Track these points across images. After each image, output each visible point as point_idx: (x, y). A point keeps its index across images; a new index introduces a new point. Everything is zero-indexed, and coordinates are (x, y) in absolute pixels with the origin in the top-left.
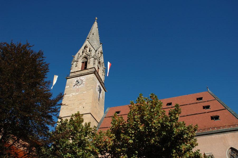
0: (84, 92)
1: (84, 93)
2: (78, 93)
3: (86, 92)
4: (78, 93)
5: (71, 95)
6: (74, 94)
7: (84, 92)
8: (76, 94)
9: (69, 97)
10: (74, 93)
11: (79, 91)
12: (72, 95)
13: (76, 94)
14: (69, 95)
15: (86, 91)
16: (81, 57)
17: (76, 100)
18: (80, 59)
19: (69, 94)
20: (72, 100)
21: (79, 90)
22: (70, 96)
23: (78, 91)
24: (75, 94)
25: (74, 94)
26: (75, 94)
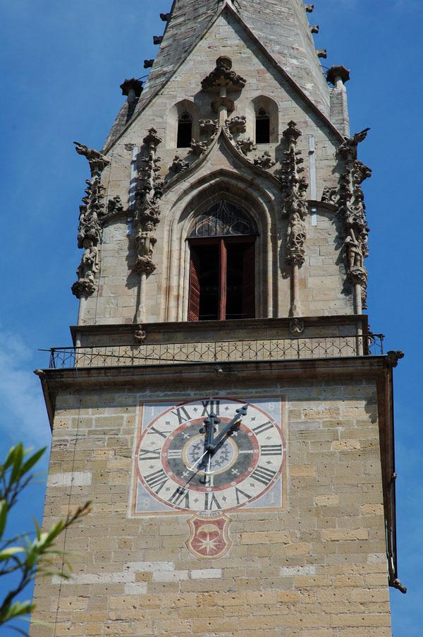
0: (290, 562)
1: (288, 582)
3: (311, 570)
4: (215, 573)
5: (129, 576)
6: (164, 570)
7: (287, 572)
8: (197, 574)
10: (169, 566)
11: (220, 546)
12: (144, 577)
13: (197, 574)
14: (105, 579)
16: (185, 185)
18: (172, 196)
21: (226, 534)
22: (118, 588)
23: (209, 544)
24: (183, 575)
25: (164, 570)
26: (183, 575)
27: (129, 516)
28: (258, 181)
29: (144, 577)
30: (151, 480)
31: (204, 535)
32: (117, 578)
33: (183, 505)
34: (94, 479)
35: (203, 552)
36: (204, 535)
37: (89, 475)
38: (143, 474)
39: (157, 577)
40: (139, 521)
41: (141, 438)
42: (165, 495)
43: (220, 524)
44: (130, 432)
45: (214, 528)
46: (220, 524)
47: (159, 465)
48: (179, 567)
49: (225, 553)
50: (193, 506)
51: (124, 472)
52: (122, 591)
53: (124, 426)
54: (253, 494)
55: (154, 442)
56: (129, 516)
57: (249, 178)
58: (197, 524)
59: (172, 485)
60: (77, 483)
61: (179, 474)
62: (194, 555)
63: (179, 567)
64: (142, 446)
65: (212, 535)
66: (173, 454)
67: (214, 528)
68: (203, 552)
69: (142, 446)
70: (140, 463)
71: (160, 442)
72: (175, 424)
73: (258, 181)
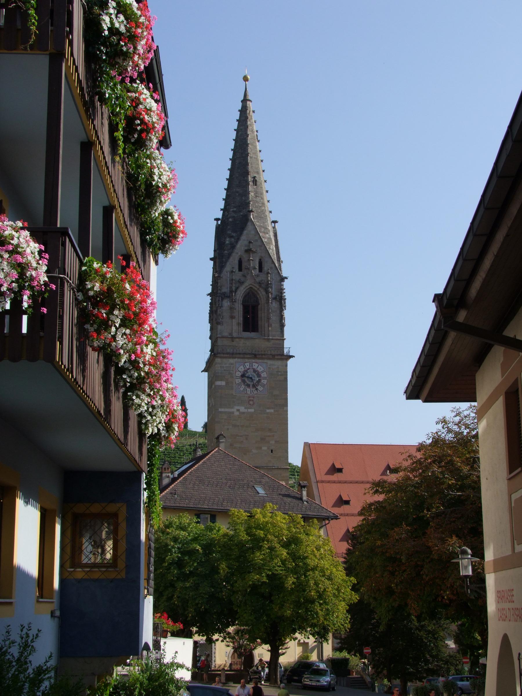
0: (269, 408)
2: (252, 410)
3: (272, 411)
4: (252, 410)
5: (234, 410)
6: (242, 409)
7: (268, 411)
8: (250, 410)
11: (254, 404)
12: (238, 410)
13: (250, 410)
15: (272, 408)
22: (233, 413)
23: (251, 403)
24: (246, 410)
25: (242, 409)
27: (234, 394)
29: (238, 410)
30: (239, 384)
31: (250, 400)
32: (231, 410)
34: (226, 384)
35: (250, 405)
36: (250, 400)
38: (237, 383)
39: (241, 411)
41: (236, 372)
42: (242, 389)
43: (254, 397)
44: (233, 371)
45: (252, 399)
46: (254, 397)
48: (245, 408)
52: (234, 414)
54: (261, 390)
58: (249, 397)
59: (243, 386)
61: (244, 383)
63: (245, 408)
64: (236, 375)
65: (252, 400)
68: (250, 405)
69: (236, 375)
70: (236, 380)
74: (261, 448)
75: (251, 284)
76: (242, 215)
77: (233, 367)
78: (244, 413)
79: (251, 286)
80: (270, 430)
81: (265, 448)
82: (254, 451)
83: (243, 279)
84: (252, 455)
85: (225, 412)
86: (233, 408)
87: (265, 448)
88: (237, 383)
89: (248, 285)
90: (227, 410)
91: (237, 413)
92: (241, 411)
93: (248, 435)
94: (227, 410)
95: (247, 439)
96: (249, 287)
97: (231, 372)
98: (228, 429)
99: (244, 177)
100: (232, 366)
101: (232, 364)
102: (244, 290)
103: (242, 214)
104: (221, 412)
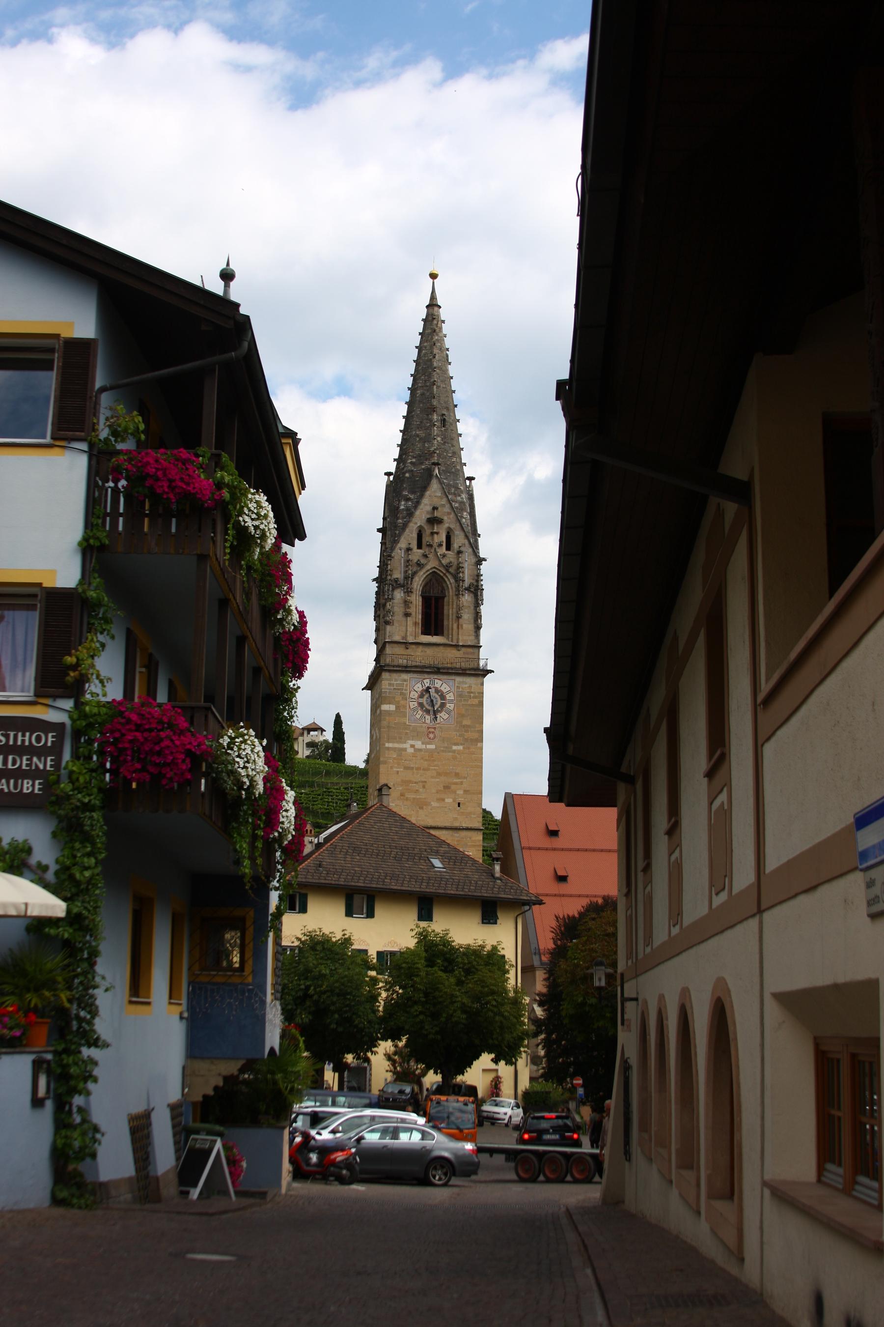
2: (432, 747)
4: (432, 747)
5: (407, 746)
6: (419, 744)
8: (429, 747)
9: (403, 753)
10: (419, 743)
11: (435, 737)
13: (429, 747)
17: (428, 769)
19: (401, 740)
20: (418, 769)
21: (437, 732)
22: (405, 749)
23: (431, 736)
24: (424, 747)
25: (419, 744)
26: (424, 747)
27: (407, 723)
28: (447, 574)
29: (412, 746)
30: (414, 710)
31: (430, 732)
33: (424, 721)
35: (430, 738)
36: (430, 732)
37: (394, 706)
39: (416, 747)
40: (410, 725)
41: (410, 693)
42: (418, 716)
43: (435, 728)
44: (406, 690)
45: (433, 730)
46: (435, 728)
47: (416, 704)
48: (423, 743)
49: (436, 740)
50: (427, 721)
51: (405, 707)
52: (406, 751)
53: (404, 688)
55: (414, 695)
56: (407, 723)
57: (444, 572)
58: (428, 728)
59: (420, 712)
60: (391, 709)
62: (427, 740)
63: (423, 743)
64: (411, 696)
65: (433, 732)
66: (421, 700)
67: (433, 730)
68: (430, 738)
69: (411, 696)
71: (416, 695)
72: (421, 689)
73: (447, 574)
74: (443, 800)
75: (434, 568)
76: (423, 469)
77: (407, 685)
78: (420, 750)
79: (434, 570)
80: (457, 775)
81: (449, 800)
82: (434, 804)
83: (423, 561)
84: (431, 810)
85: (394, 749)
86: (405, 743)
87: (449, 800)
88: (412, 707)
89: (429, 568)
90: (396, 745)
91: (411, 750)
92: (416, 747)
93: (425, 782)
94: (396, 745)
95: (424, 787)
96: (431, 571)
97: (404, 691)
98: (398, 772)
99: (427, 415)
100: (405, 683)
101: (405, 681)
102: (425, 576)
103: (423, 467)
104: (388, 748)
